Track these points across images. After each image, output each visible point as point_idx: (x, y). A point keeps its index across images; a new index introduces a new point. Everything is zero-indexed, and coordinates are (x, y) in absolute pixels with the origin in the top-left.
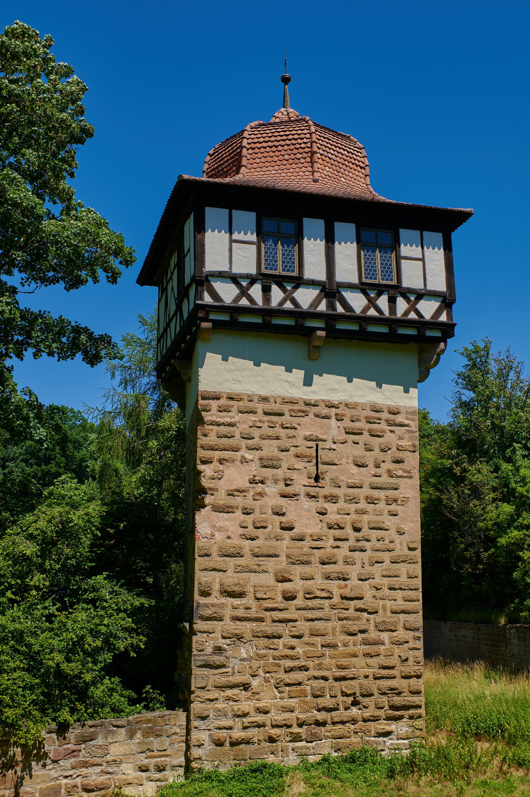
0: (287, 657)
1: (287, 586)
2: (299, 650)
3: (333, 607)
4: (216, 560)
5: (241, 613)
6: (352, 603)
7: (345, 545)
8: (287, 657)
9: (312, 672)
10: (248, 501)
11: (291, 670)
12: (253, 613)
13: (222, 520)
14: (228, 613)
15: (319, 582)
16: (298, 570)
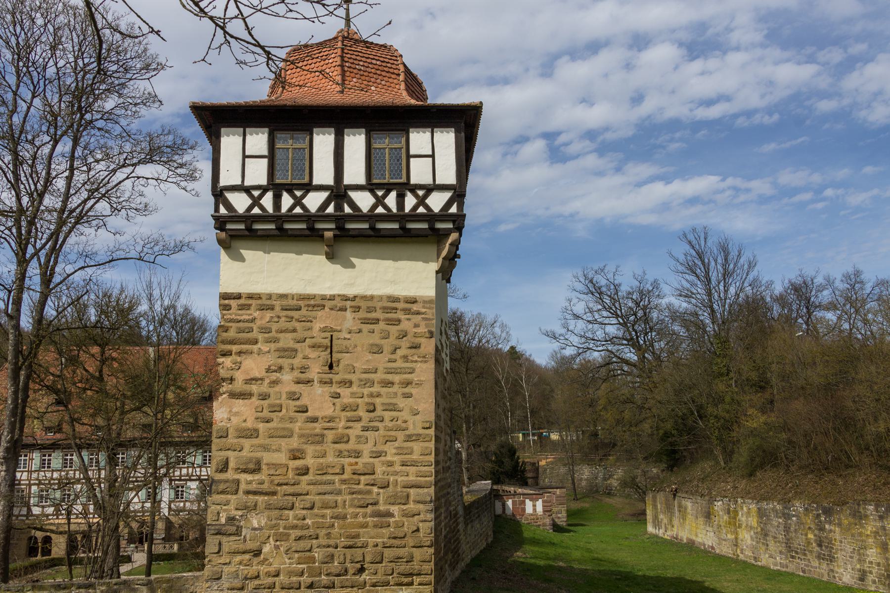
0: (295, 527)
1: (298, 463)
2: (309, 521)
3: (343, 482)
4: (231, 440)
5: (254, 487)
6: (362, 478)
7: (359, 425)
8: (295, 527)
9: (323, 541)
10: (264, 388)
11: (299, 538)
12: (265, 487)
13: (239, 405)
14: (243, 487)
15: (330, 459)
16: (310, 449)
